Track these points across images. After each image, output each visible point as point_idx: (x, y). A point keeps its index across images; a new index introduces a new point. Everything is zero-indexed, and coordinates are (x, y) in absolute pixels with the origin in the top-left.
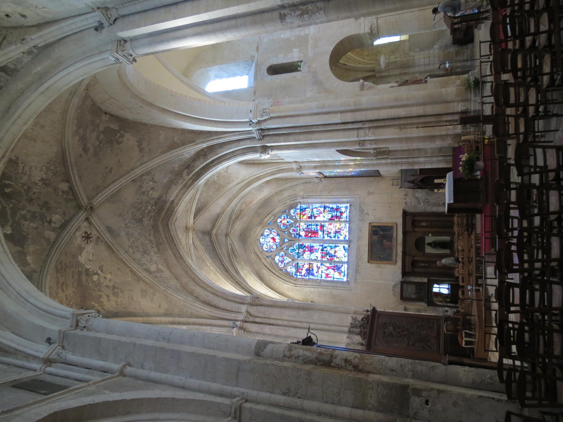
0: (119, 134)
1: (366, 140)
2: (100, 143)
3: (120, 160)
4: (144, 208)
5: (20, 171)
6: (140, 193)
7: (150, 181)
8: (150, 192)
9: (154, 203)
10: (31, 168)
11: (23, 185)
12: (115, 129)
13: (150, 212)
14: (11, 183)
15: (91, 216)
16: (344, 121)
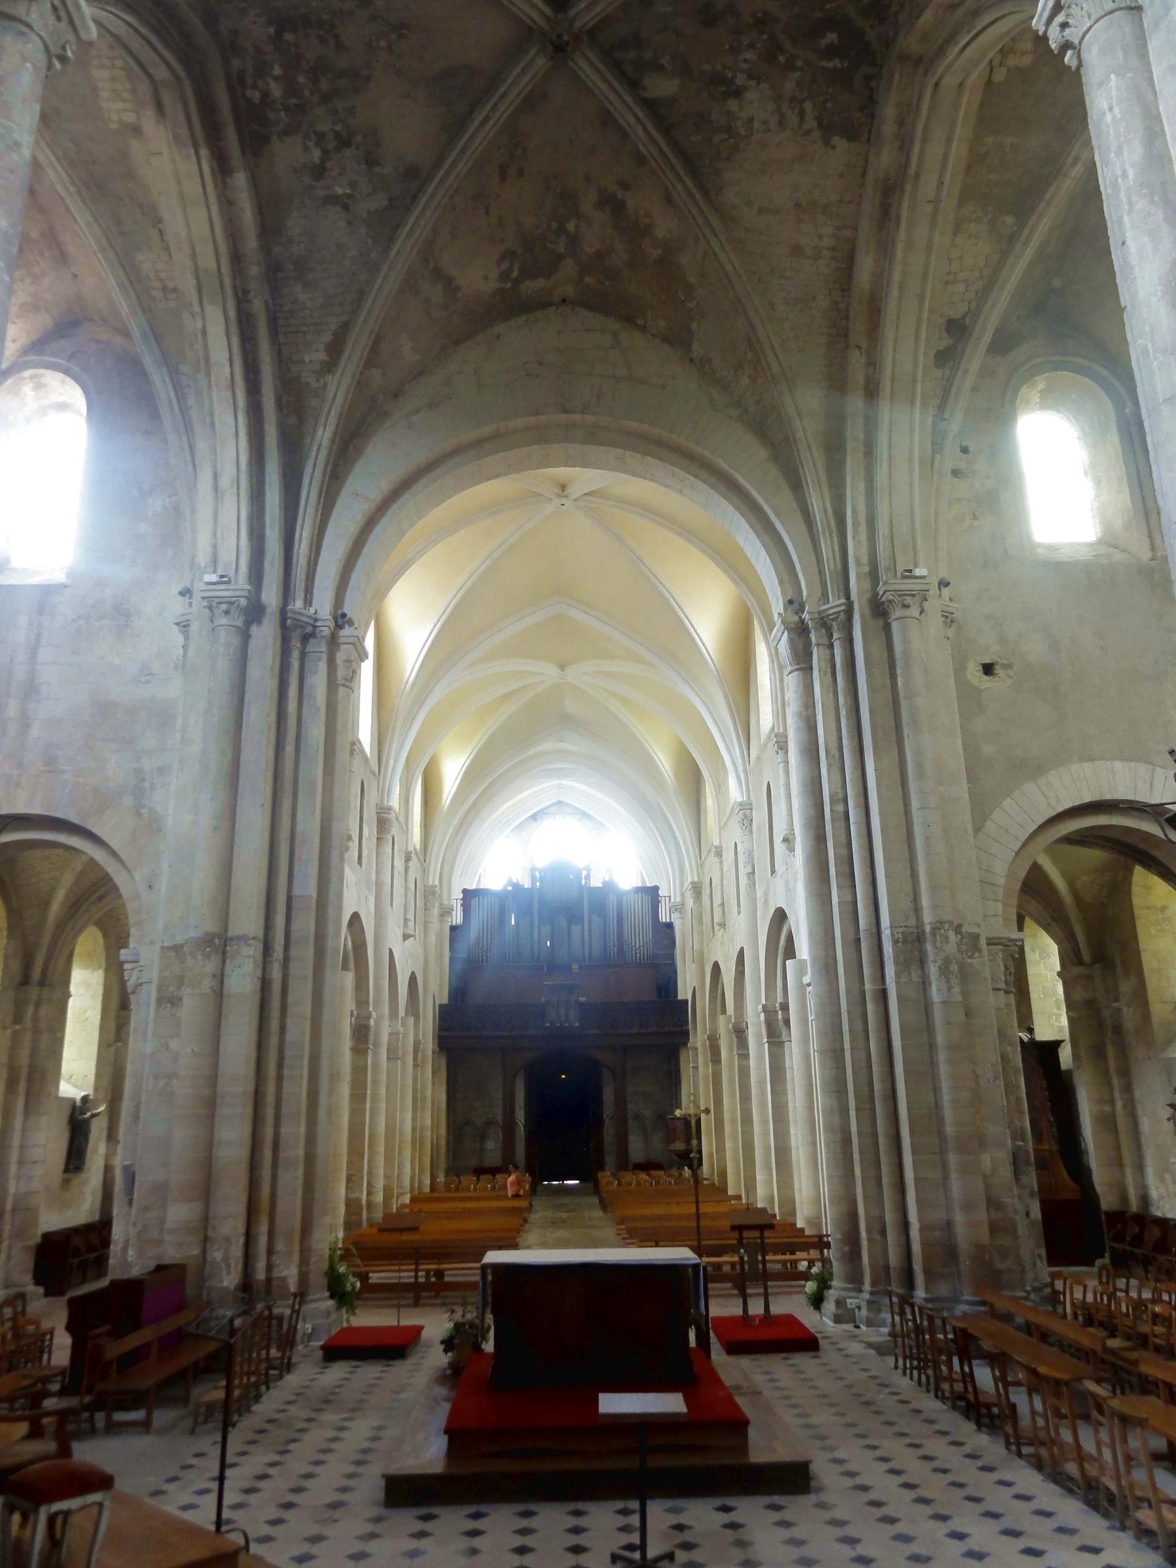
0: (515, 274)
1: (224, 962)
2: (561, 229)
3: (487, 213)
4: (301, 79)
5: (808, 106)
6: (359, 138)
7: (349, 196)
8: (317, 154)
9: (272, 115)
10: (781, 123)
11: (789, 67)
12: (528, 283)
13: (261, 70)
14: (823, 63)
15: (548, 18)
16: (296, 903)
